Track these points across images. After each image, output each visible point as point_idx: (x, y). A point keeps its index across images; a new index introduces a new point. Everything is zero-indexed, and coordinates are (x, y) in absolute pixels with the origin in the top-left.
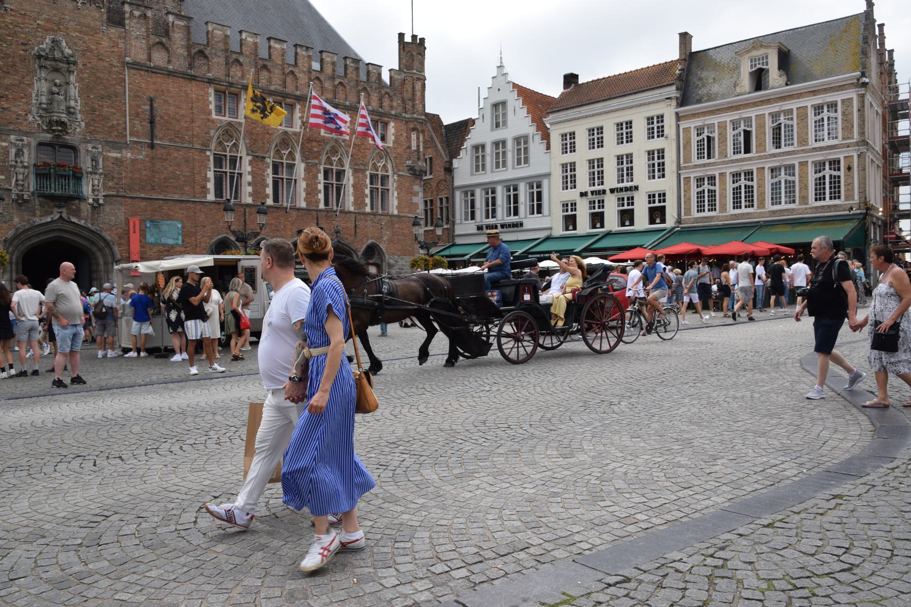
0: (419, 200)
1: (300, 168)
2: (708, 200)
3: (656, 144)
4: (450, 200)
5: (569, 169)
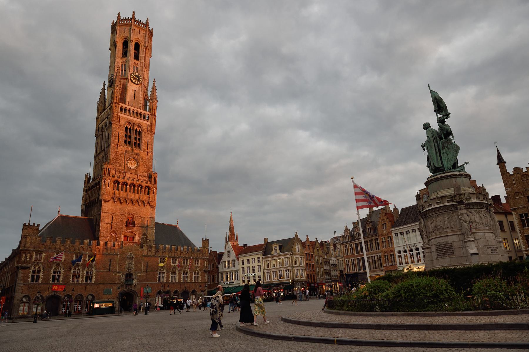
0: (206, 278)
1: (177, 273)
2: (269, 277)
3: (259, 264)
4: (218, 275)
5: (243, 268)
